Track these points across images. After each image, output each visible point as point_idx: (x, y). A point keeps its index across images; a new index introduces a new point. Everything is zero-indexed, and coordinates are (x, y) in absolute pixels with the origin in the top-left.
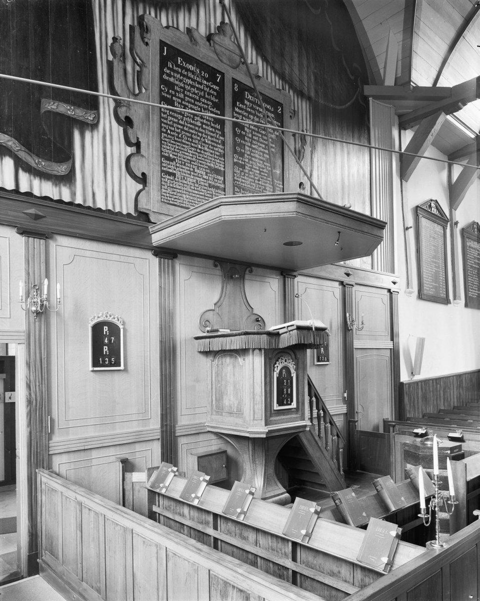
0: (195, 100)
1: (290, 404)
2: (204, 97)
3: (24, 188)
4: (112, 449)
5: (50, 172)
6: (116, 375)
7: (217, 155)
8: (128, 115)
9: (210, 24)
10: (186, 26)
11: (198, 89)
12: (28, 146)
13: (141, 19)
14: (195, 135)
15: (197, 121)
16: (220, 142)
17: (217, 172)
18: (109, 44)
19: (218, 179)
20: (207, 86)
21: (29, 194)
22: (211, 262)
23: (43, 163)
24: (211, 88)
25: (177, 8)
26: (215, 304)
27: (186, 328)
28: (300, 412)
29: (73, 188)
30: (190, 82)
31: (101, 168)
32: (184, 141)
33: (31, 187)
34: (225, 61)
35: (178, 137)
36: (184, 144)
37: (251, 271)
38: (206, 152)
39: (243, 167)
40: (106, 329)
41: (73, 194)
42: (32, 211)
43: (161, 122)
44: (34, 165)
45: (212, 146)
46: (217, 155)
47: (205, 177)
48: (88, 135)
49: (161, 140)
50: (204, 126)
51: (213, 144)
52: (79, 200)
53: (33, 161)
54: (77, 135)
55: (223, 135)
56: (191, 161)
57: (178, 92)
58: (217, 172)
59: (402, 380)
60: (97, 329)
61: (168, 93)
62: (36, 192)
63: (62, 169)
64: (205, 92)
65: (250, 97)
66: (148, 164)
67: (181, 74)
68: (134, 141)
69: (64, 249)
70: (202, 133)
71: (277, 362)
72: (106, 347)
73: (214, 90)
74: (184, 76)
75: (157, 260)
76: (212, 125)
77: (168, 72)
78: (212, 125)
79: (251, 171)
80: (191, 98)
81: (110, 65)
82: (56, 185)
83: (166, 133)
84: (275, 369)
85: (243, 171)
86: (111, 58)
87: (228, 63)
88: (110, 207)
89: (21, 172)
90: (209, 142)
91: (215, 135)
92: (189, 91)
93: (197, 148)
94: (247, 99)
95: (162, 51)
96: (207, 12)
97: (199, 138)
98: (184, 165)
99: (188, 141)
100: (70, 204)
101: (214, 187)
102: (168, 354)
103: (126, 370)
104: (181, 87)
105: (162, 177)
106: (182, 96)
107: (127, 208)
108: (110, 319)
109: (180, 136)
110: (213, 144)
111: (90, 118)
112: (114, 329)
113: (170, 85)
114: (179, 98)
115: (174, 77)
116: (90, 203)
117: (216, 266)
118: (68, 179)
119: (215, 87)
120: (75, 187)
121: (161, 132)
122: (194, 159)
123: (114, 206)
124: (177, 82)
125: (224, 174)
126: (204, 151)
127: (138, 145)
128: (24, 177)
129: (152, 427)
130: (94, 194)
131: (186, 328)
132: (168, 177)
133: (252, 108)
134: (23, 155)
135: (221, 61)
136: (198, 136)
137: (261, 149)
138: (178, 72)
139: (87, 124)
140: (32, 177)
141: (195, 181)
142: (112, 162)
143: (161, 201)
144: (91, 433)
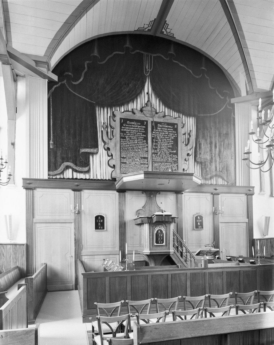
0: (134, 134)
1: (162, 243)
2: (139, 132)
3: (75, 177)
4: (102, 256)
5: (82, 171)
6: (103, 232)
7: (144, 152)
8: (108, 147)
9: (142, 104)
10: (132, 108)
11: (136, 130)
12: (76, 165)
13: (113, 113)
14: (135, 147)
15: (135, 142)
16: (146, 147)
17: (145, 158)
18: (102, 125)
19: (145, 161)
20: (140, 128)
21: (76, 179)
22: (141, 192)
23: (80, 168)
24: (141, 128)
25: (128, 103)
26: (143, 207)
27: (130, 216)
28: (168, 247)
29: (90, 174)
30: (133, 128)
31: (100, 166)
32: (130, 150)
33: (77, 176)
34: (148, 116)
35: (127, 149)
36: (130, 151)
37: (159, 194)
38: (140, 152)
39: (157, 153)
40: (99, 218)
41: (90, 176)
42: (76, 184)
43: (121, 146)
44: (78, 169)
45: (142, 149)
46: (144, 152)
47: (139, 161)
48: (95, 156)
49: (121, 152)
50: (139, 143)
51: (142, 148)
52: (92, 178)
53: (77, 168)
54: (91, 157)
55: (147, 143)
56: (133, 157)
57: (127, 133)
58: (145, 158)
59: (254, 237)
60: (97, 218)
61: (123, 135)
62: (78, 178)
63: (86, 169)
64: (139, 130)
65: (160, 126)
66: (116, 161)
67: (129, 127)
68: (110, 155)
69: (86, 194)
70: (138, 145)
71: (156, 228)
72: (100, 223)
73: (143, 128)
74: (130, 127)
75: (118, 193)
76: (142, 141)
77: (123, 128)
78: (142, 141)
79: (161, 154)
80: (133, 134)
81: (102, 131)
82: (84, 174)
83: (123, 149)
84: (155, 230)
85: (157, 155)
86: (102, 129)
87: (150, 116)
88: (102, 178)
89: (74, 172)
90: (141, 148)
91: (143, 145)
92: (132, 132)
93: (135, 151)
94: (158, 127)
95: (121, 121)
96: (141, 99)
97: (136, 148)
98: (130, 159)
99: (131, 150)
100: (89, 179)
101: (143, 164)
102: (123, 226)
103: (106, 230)
104: (129, 131)
105: (121, 165)
106: (129, 134)
107: (108, 177)
108: (101, 214)
109: (128, 149)
110: (142, 148)
111: (95, 151)
112: (102, 218)
113: (124, 132)
114: (128, 135)
115: (126, 129)
116: (95, 178)
117: (143, 193)
118: (88, 171)
119: (143, 127)
120: (90, 174)
121: (121, 149)
122: (134, 156)
123: (103, 177)
124: (126, 130)
125: (147, 158)
126: (139, 152)
127: (112, 155)
128: (75, 173)
129: (116, 250)
130: (96, 175)
131: (130, 216)
132: (123, 164)
133: (161, 130)
134: (75, 167)
135: (146, 116)
136: (136, 147)
137: (166, 145)
138: (127, 127)
139: (95, 153)
140: (77, 173)
141: (135, 163)
142: (103, 163)
143: (121, 173)
144: (95, 250)
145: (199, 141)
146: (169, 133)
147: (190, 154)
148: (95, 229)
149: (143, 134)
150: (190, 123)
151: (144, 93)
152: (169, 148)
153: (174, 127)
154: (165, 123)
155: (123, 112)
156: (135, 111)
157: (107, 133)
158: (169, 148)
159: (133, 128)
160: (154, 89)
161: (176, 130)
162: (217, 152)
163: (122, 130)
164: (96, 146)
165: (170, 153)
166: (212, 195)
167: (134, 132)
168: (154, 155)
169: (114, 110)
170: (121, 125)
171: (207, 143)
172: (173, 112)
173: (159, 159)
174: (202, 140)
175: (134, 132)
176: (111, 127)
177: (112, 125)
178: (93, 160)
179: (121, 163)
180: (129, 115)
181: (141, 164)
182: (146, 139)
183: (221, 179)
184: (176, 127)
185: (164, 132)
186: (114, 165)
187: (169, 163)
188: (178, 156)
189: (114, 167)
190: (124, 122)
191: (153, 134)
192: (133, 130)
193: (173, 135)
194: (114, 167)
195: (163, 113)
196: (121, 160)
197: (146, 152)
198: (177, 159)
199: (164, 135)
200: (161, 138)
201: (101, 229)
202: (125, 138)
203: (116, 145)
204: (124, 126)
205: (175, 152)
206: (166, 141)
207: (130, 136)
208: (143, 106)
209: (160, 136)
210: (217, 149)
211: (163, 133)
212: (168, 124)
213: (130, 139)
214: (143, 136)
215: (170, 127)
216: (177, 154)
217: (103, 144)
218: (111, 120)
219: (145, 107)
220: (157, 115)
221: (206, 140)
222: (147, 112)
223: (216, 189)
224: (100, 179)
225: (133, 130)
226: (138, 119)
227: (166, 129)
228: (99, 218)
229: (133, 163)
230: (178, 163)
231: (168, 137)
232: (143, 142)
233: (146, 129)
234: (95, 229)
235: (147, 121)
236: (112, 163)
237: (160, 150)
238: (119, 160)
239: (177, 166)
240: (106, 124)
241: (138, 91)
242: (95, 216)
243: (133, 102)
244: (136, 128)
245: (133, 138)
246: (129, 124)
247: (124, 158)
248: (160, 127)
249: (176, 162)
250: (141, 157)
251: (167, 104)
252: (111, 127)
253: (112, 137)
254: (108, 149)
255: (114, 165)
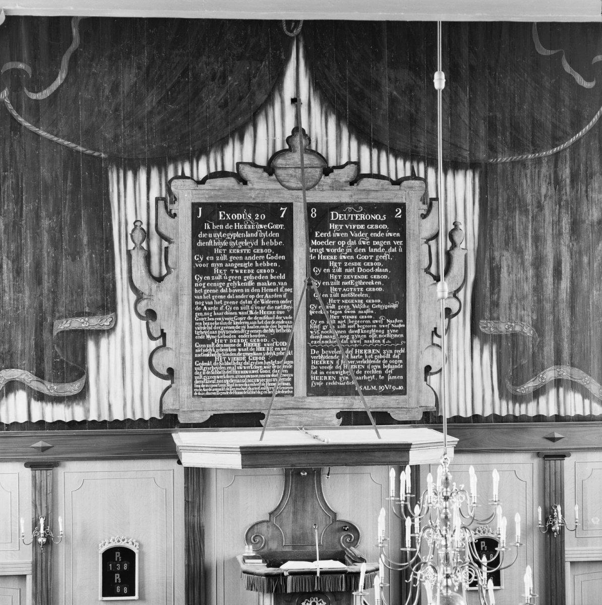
0: (244, 255)
2: (259, 246)
30: (238, 235)
40: (118, 555)
41: (87, 411)
43: (194, 300)
48: (104, 341)
49: (194, 322)
52: (93, 417)
55: (291, 284)
65: (339, 216)
66: (178, 354)
70: (255, 294)
73: (275, 231)
74: (228, 231)
86: (131, 245)
88: (129, 416)
92: (236, 247)
95: (194, 213)
101: (274, 358)
103: (142, 598)
106: (224, 257)
107: (150, 411)
108: (122, 544)
111: (106, 322)
112: (127, 555)
113: (209, 251)
116: (105, 417)
121: (194, 312)
123: (134, 413)
127: (163, 335)
133: (344, 230)
138: (218, 231)
139: (103, 331)
142: (132, 365)
145: (492, 259)
146: (372, 239)
147: (454, 311)
148: (104, 595)
149: (276, 250)
150: (459, 192)
151: (282, 102)
152: (373, 295)
153: (394, 217)
154: (356, 206)
155: (203, 182)
156: (247, 172)
157: (148, 258)
158: (373, 295)
159: (238, 235)
160: (317, 84)
161: (399, 226)
162: (564, 295)
163: (200, 244)
164: (108, 305)
165: (377, 313)
166: (537, 462)
167: (244, 247)
168: (314, 325)
169: (171, 175)
170: (197, 227)
171: (523, 263)
172: (392, 159)
173: (333, 337)
174: (505, 253)
175: (244, 247)
176: (162, 237)
177: (163, 230)
178: (98, 357)
179: (194, 359)
180: (223, 190)
181: (268, 359)
182: (286, 268)
183: (579, 397)
184: (398, 215)
185: (353, 239)
186: (171, 371)
187: (372, 348)
188: (405, 322)
189: (171, 373)
190: (205, 216)
191: (314, 247)
192: (239, 239)
193: (386, 247)
194: (171, 373)
195: (347, 173)
196: (194, 349)
197: (287, 314)
198: (403, 331)
199: (354, 247)
200: (344, 261)
201: (121, 594)
202: (209, 271)
203: (176, 299)
204: (207, 231)
205: (395, 306)
206: (360, 270)
207: (228, 262)
208: (279, 148)
209: (338, 254)
210: (565, 284)
211: (351, 243)
212: (370, 208)
213: (229, 274)
214: (277, 257)
215: (375, 217)
216: (401, 314)
217: (133, 297)
218: (162, 210)
219: (283, 152)
220: (327, 180)
221: (520, 252)
222: (291, 171)
223: (553, 440)
224: (121, 419)
225: (239, 239)
226: (258, 201)
227: (362, 227)
228: (118, 555)
229: (237, 359)
230: (405, 346)
231: (367, 253)
232: (277, 281)
233: (287, 235)
234: (104, 595)
235: (290, 206)
236: (164, 361)
237: (337, 305)
238: (187, 349)
239: (404, 357)
240: (145, 227)
241: (260, 98)
242: (102, 550)
243: (242, 139)
244: (251, 231)
245: (239, 268)
246: (224, 223)
247: (205, 341)
248: (337, 222)
249: (400, 343)
250: (270, 337)
251: (364, 133)
252: (162, 237)
253: (164, 272)
254: (151, 315)
255: (171, 371)
